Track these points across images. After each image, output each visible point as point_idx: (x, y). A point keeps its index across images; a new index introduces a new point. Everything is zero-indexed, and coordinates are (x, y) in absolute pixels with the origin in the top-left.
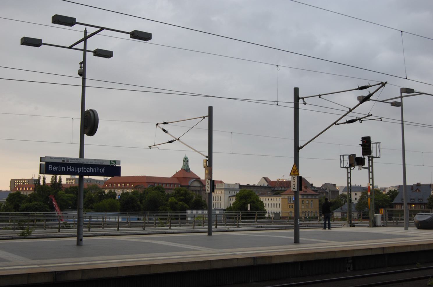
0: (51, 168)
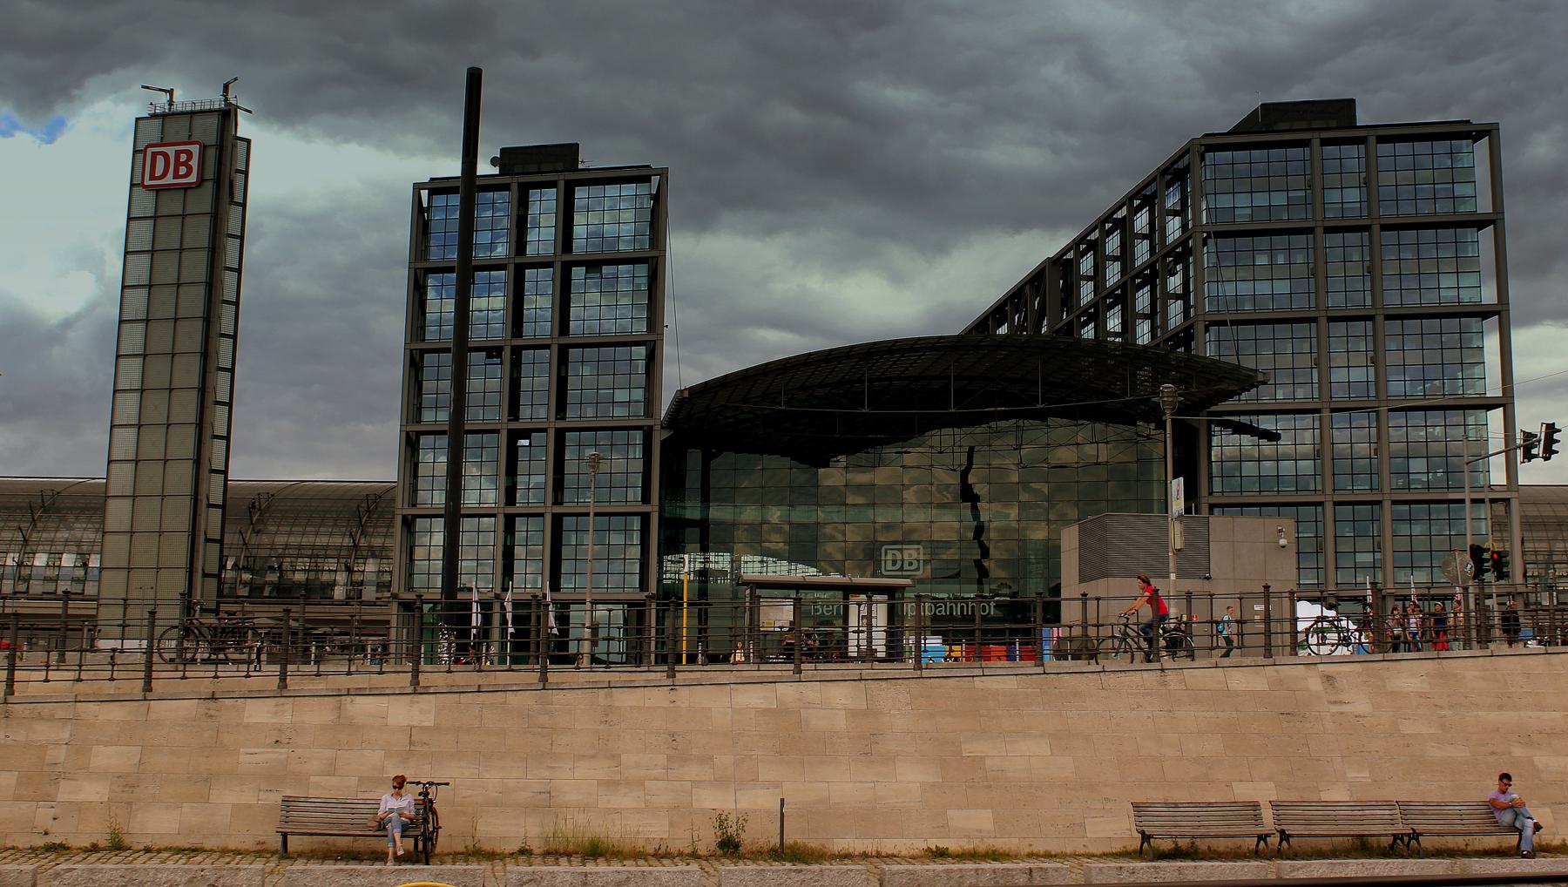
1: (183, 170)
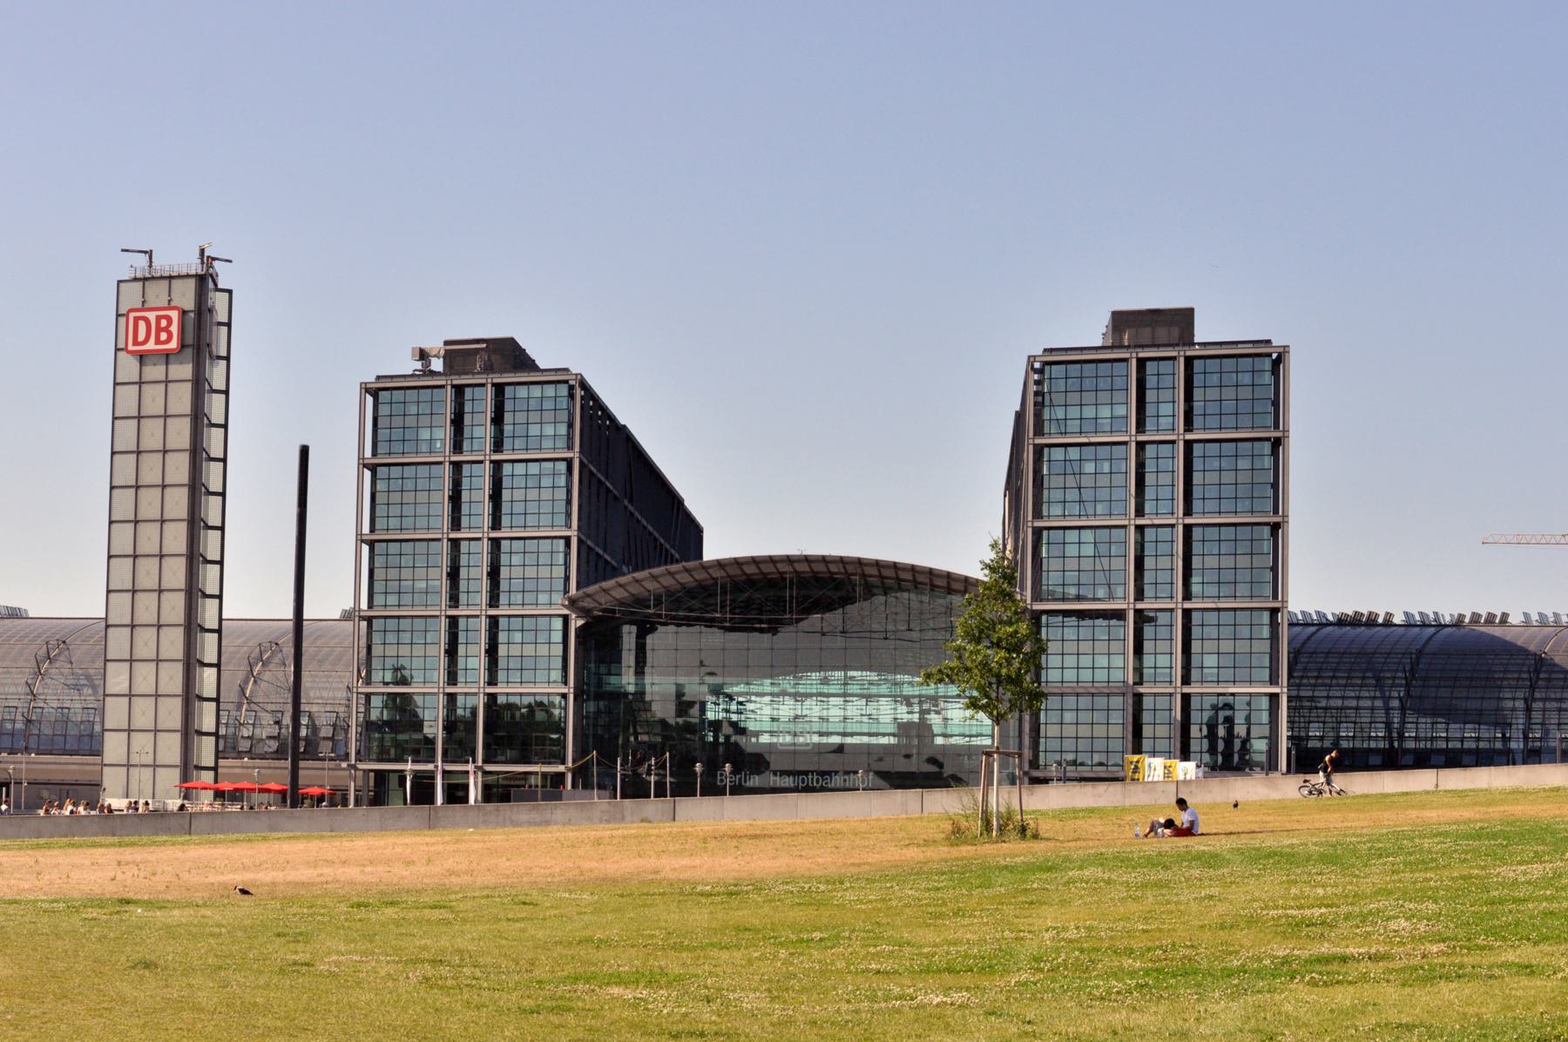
1: (164, 336)
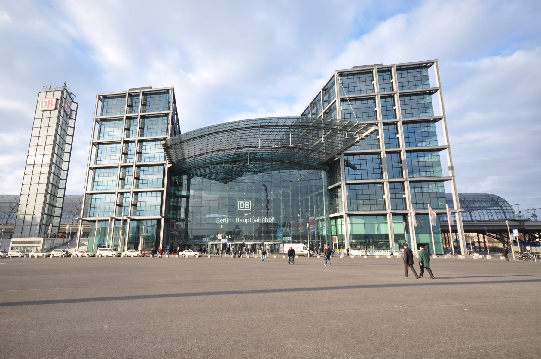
0: (219, 220)
1: (50, 105)
